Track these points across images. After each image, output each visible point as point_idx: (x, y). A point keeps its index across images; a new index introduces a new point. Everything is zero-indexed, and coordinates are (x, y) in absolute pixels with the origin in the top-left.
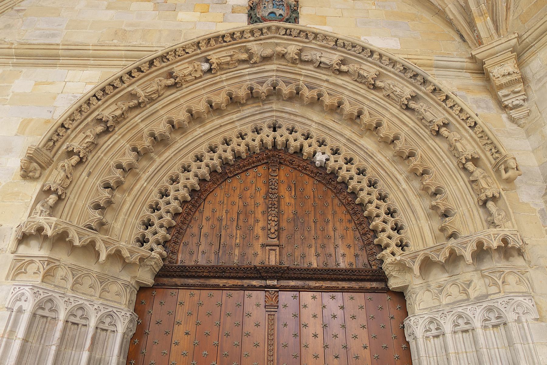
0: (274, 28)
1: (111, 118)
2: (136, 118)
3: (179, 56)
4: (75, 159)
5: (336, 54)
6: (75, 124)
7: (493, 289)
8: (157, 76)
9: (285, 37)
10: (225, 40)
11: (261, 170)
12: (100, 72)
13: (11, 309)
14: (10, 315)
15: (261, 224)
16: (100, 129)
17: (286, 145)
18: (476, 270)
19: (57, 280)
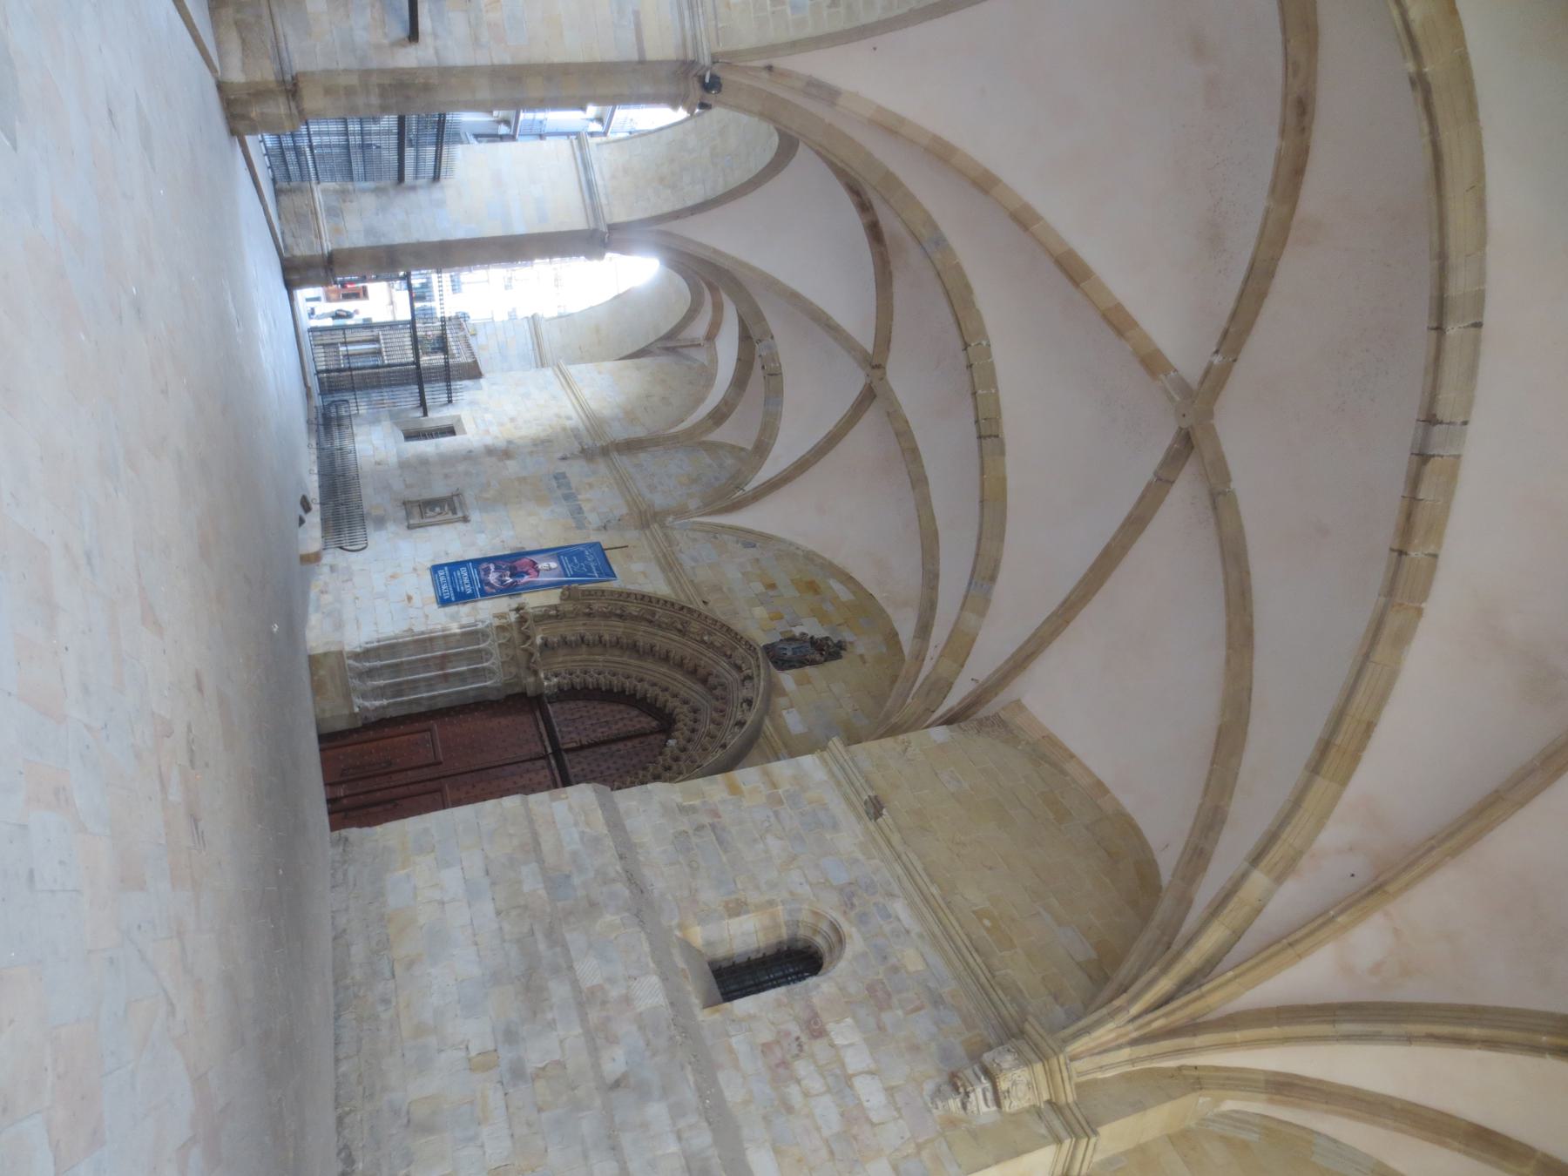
2: (643, 627)
6: (610, 597)
13: (476, 621)
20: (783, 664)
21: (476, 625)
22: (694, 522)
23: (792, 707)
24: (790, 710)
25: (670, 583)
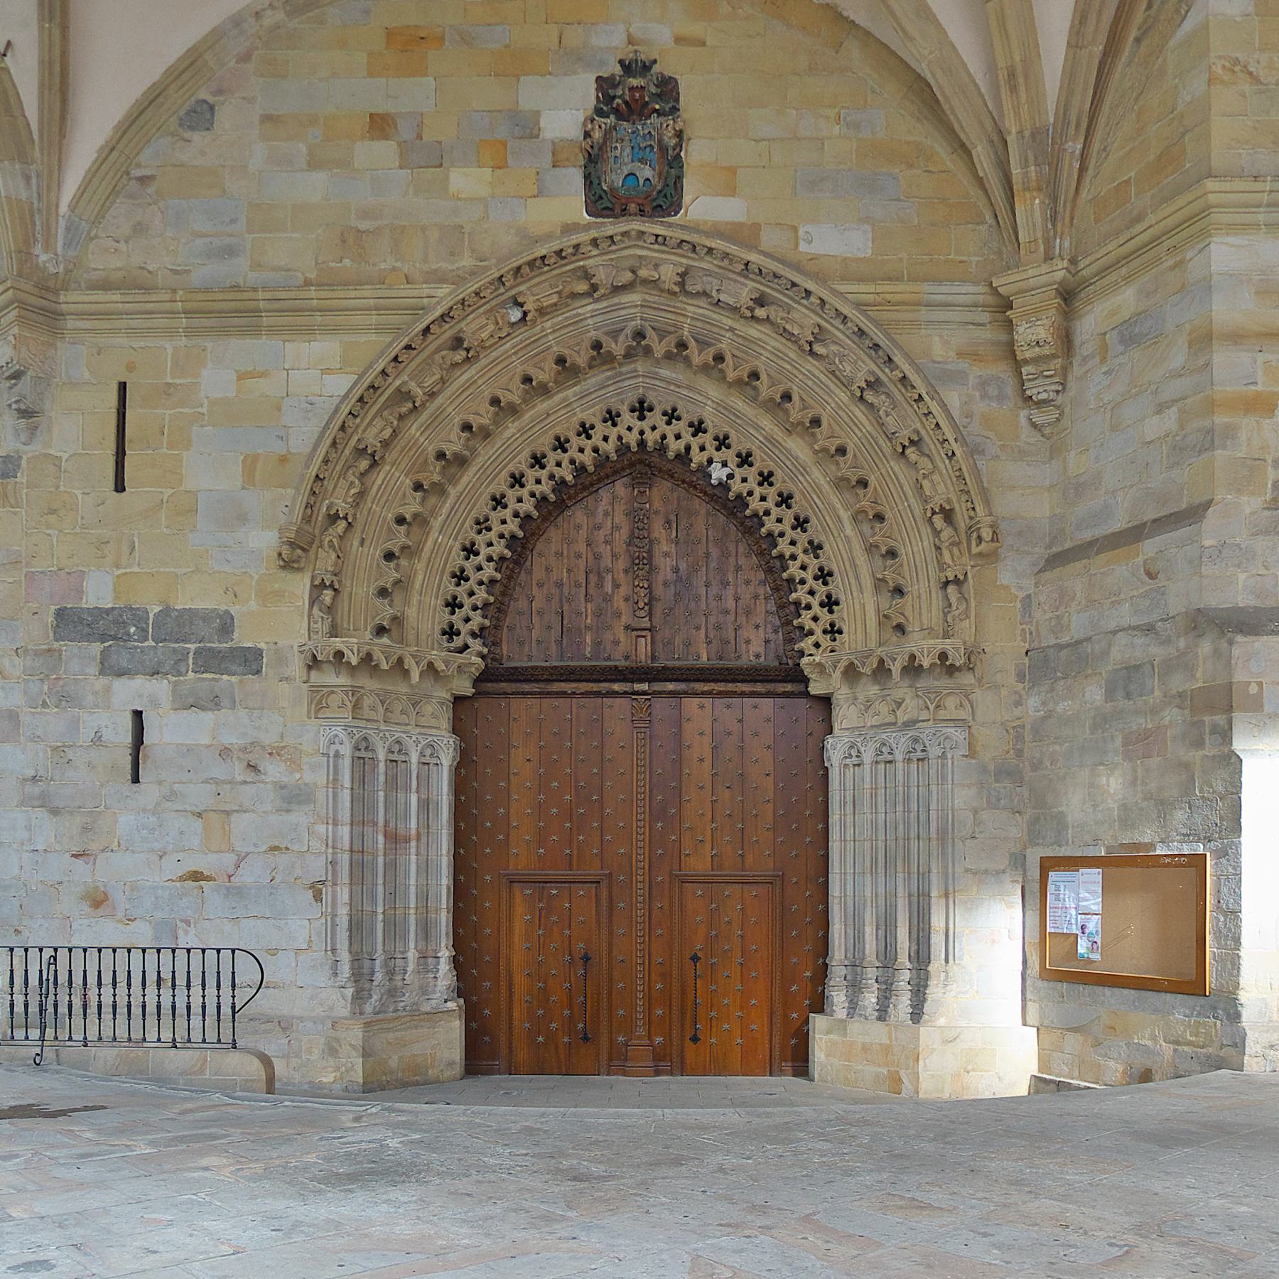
0: (633, 233)
1: (379, 445)
3: (469, 306)
4: (342, 525)
5: (746, 285)
7: (924, 715)
8: (438, 350)
9: (656, 247)
10: (546, 262)
11: (620, 488)
12: (338, 344)
14: (328, 761)
15: (623, 591)
16: (364, 464)
17: (662, 448)
18: (910, 687)
19: (367, 713)
20: (665, 196)
21: (337, 755)
22: (73, 207)
23: (795, 229)
24: (801, 233)
25: (308, 332)
